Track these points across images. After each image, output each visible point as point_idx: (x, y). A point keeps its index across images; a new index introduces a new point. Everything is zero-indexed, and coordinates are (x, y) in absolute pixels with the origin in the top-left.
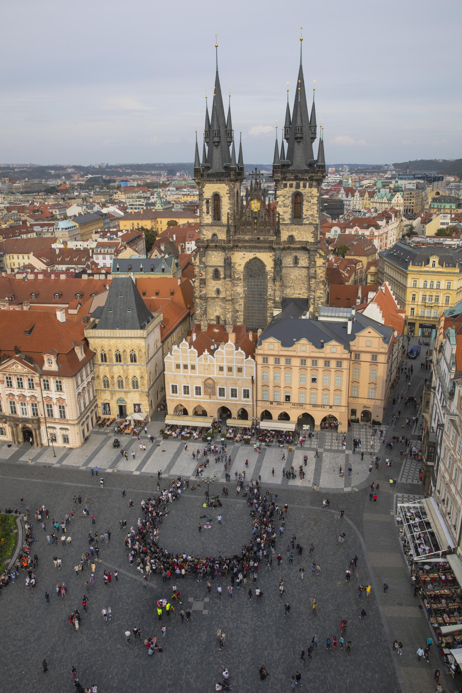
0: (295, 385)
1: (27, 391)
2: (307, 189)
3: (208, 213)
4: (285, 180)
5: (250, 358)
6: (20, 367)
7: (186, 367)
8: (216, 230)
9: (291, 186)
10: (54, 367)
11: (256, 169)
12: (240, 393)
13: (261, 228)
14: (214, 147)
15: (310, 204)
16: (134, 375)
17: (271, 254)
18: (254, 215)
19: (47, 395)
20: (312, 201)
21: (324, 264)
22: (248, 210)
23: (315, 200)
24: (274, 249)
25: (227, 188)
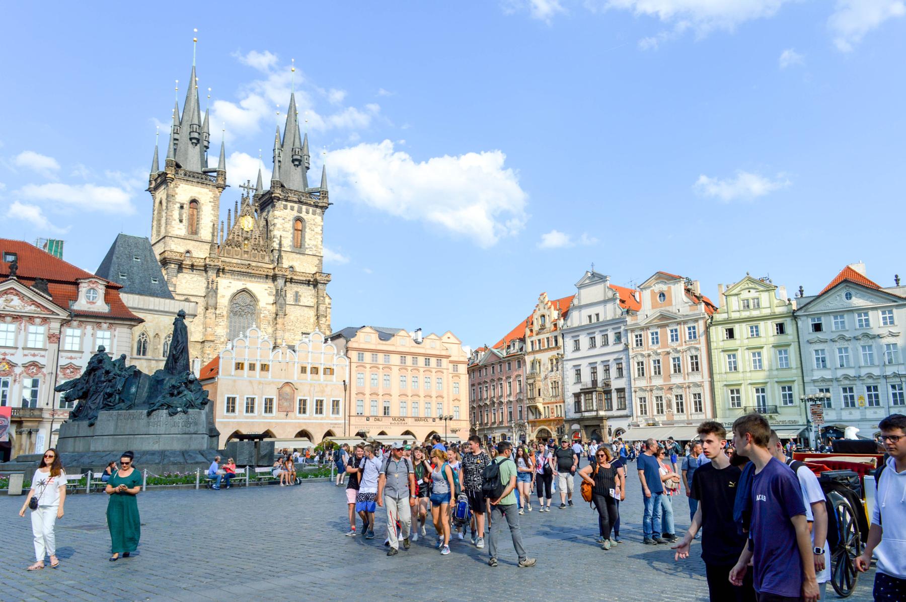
0: (395, 392)
1: (20, 352)
3: (181, 221)
4: (287, 200)
5: (342, 354)
6: (16, 302)
7: (252, 367)
8: (190, 245)
10: (101, 306)
14: (190, 145)
17: (266, 286)
18: (244, 235)
19: (69, 361)
20: (316, 230)
24: (274, 278)
25: (211, 195)
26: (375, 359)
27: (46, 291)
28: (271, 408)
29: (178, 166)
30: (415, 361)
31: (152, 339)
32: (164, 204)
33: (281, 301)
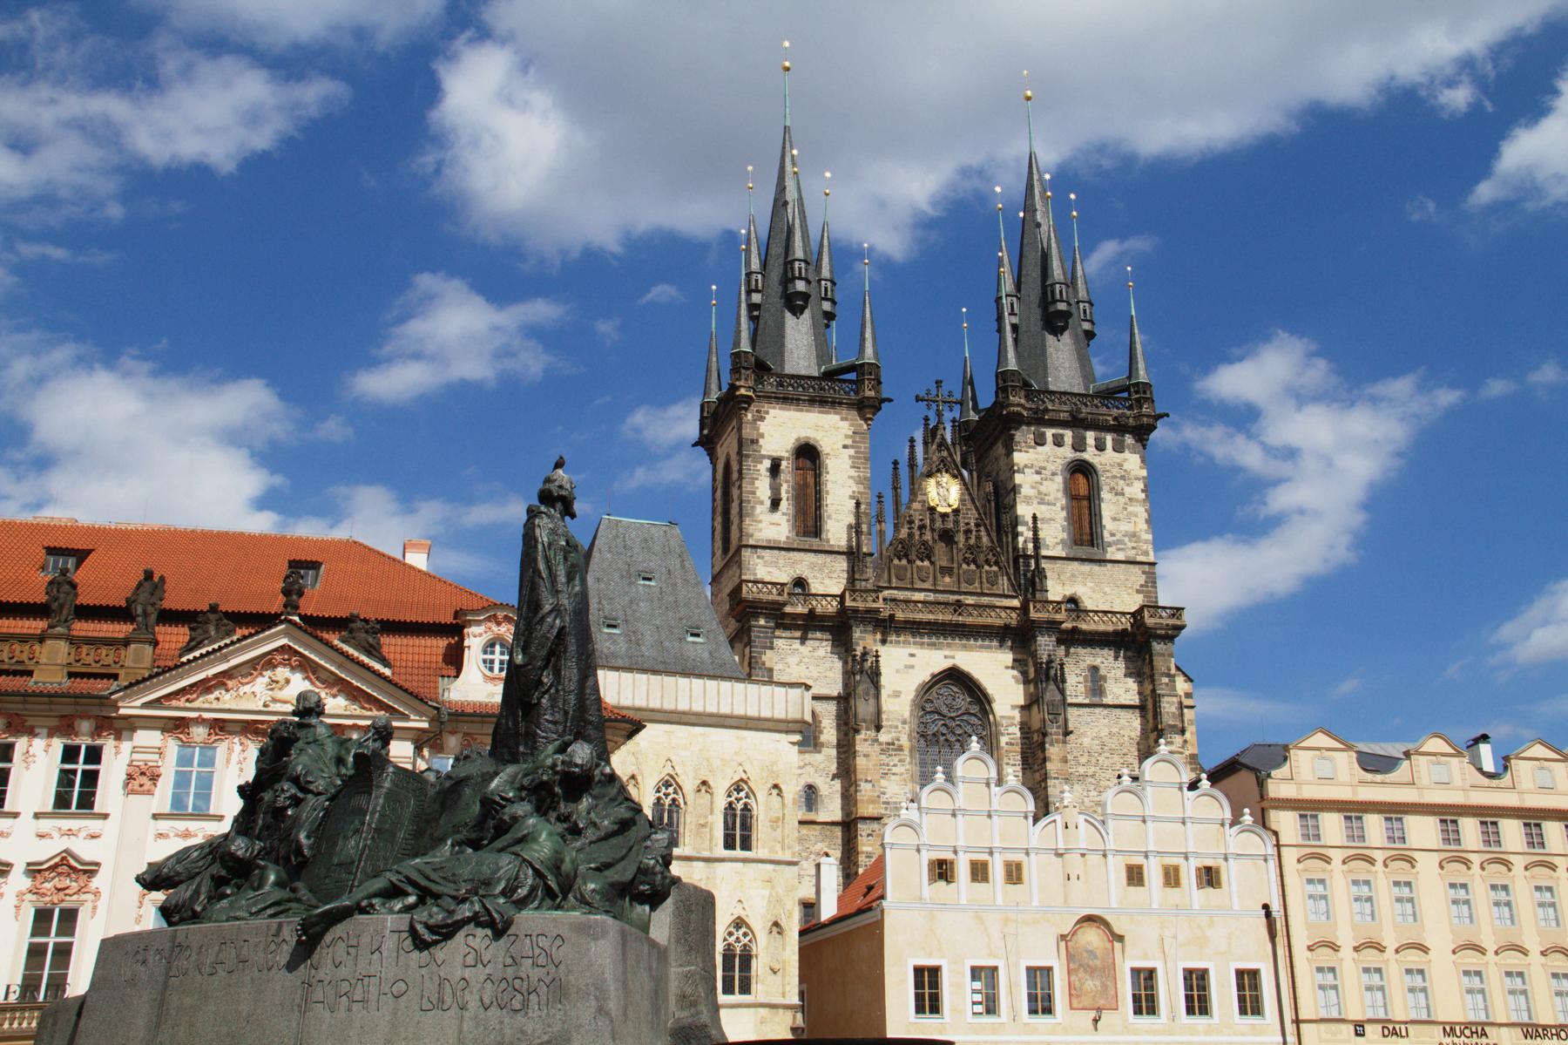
2: (1109, 454)
3: (775, 504)
5: (1248, 819)
7: (979, 872)
8: (803, 565)
9: (1058, 442)
11: (938, 383)
12: (1223, 992)
13: (964, 566)
14: (788, 315)
15: (1122, 500)
16: (738, 912)
18: (938, 524)
20: (1127, 490)
21: (1188, 695)
22: (916, 505)
23: (1136, 490)
26: (1356, 834)
27: (373, 651)
28: (1049, 998)
29: (761, 369)
30: (1491, 835)
31: (690, 797)
32: (735, 467)
33: (1051, 693)
